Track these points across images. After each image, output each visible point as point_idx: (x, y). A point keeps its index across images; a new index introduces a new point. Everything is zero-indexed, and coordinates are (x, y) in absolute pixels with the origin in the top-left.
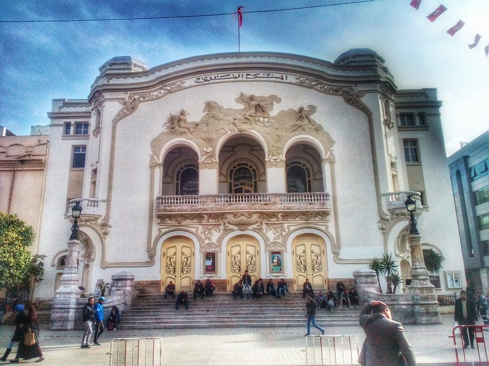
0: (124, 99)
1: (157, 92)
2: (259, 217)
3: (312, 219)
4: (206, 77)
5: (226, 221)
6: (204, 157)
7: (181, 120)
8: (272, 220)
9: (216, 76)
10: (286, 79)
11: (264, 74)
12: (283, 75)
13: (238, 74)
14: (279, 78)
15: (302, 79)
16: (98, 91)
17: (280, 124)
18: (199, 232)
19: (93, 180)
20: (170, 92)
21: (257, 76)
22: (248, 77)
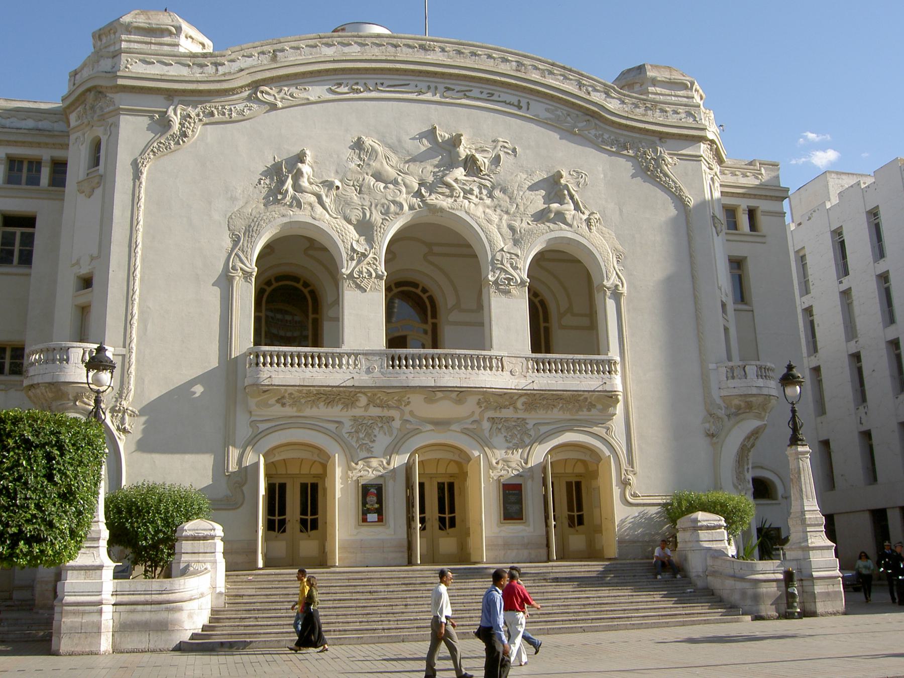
1: (244, 104)
2: (478, 403)
3: (585, 410)
5: (407, 409)
8: (503, 410)
9: (379, 82)
11: (482, 93)
12: (521, 99)
13: (428, 84)
14: (513, 105)
15: (561, 114)
16: (95, 87)
18: (344, 431)
19: (82, 300)
21: (467, 94)
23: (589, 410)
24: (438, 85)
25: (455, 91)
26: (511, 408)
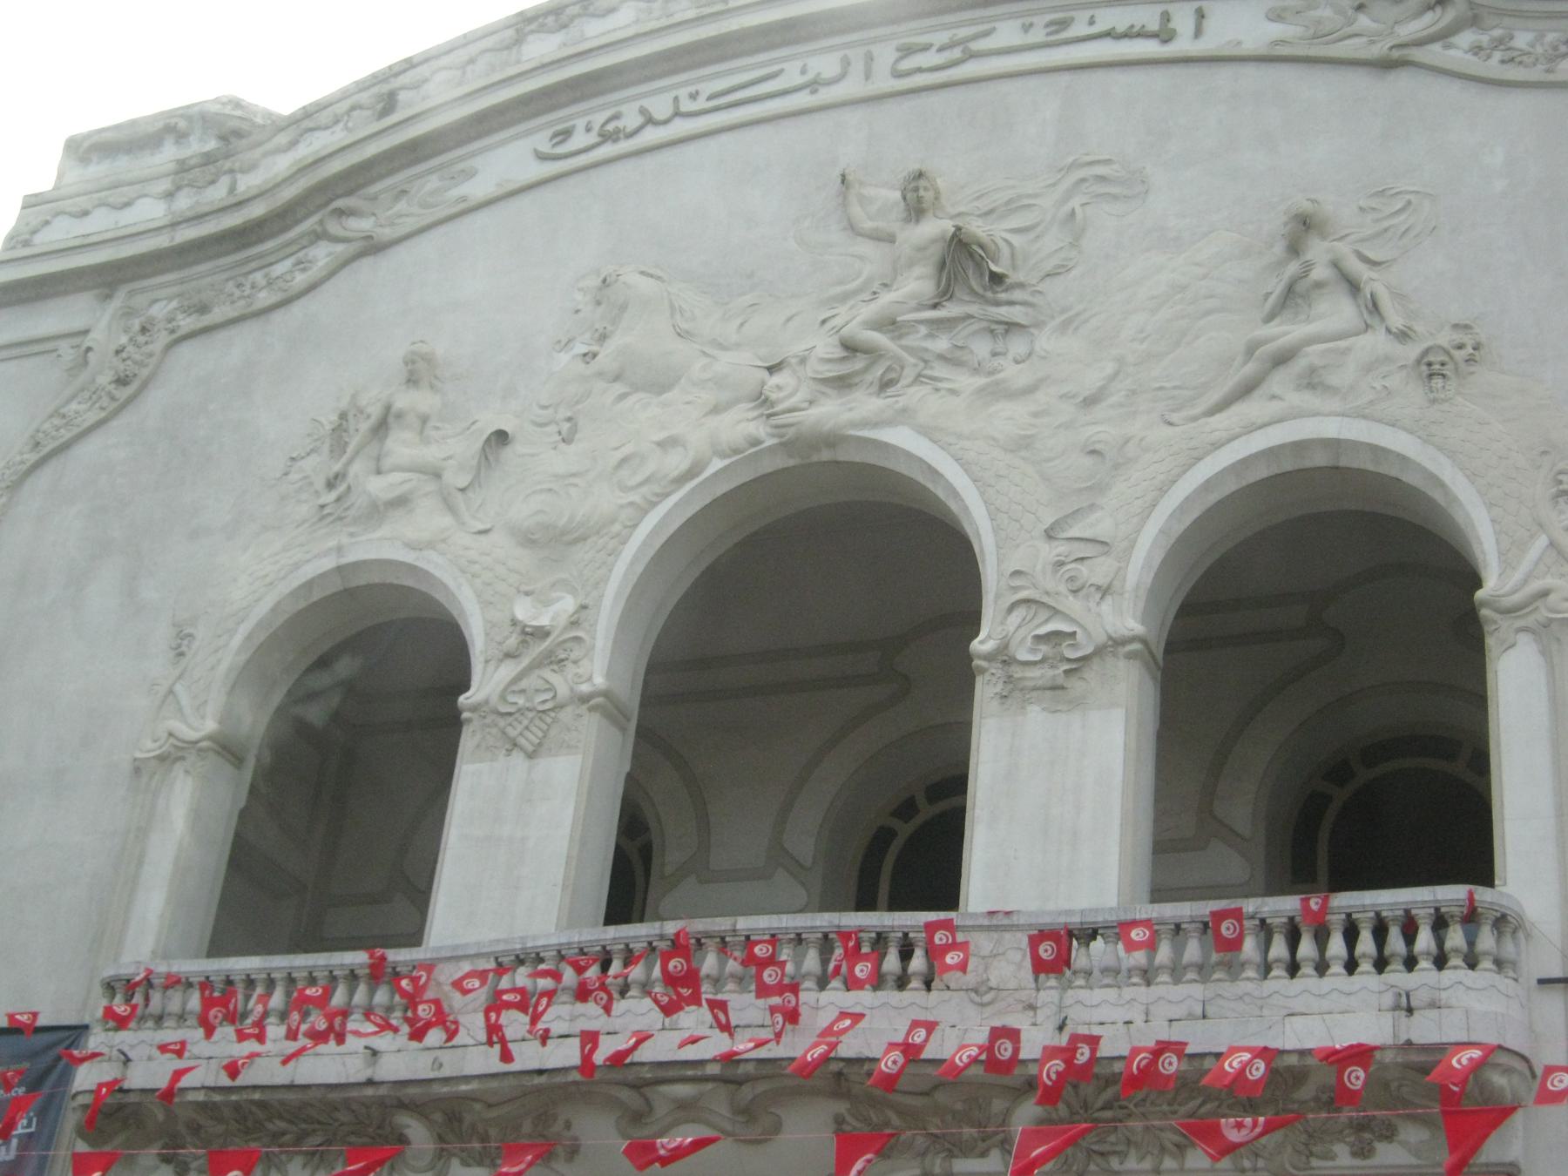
0: (86, 332)
1: (288, 263)
4: (616, 117)
6: (507, 671)
7: (400, 416)
9: (683, 93)
10: (1198, 33)
11: (1027, 28)
13: (839, 55)
14: (1142, 34)
17: (1120, 361)
20: (373, 248)
21: (976, 46)
22: (906, 65)
23: (1363, 1152)
24: (876, 50)
25: (934, 49)
26: (995, 1154)
